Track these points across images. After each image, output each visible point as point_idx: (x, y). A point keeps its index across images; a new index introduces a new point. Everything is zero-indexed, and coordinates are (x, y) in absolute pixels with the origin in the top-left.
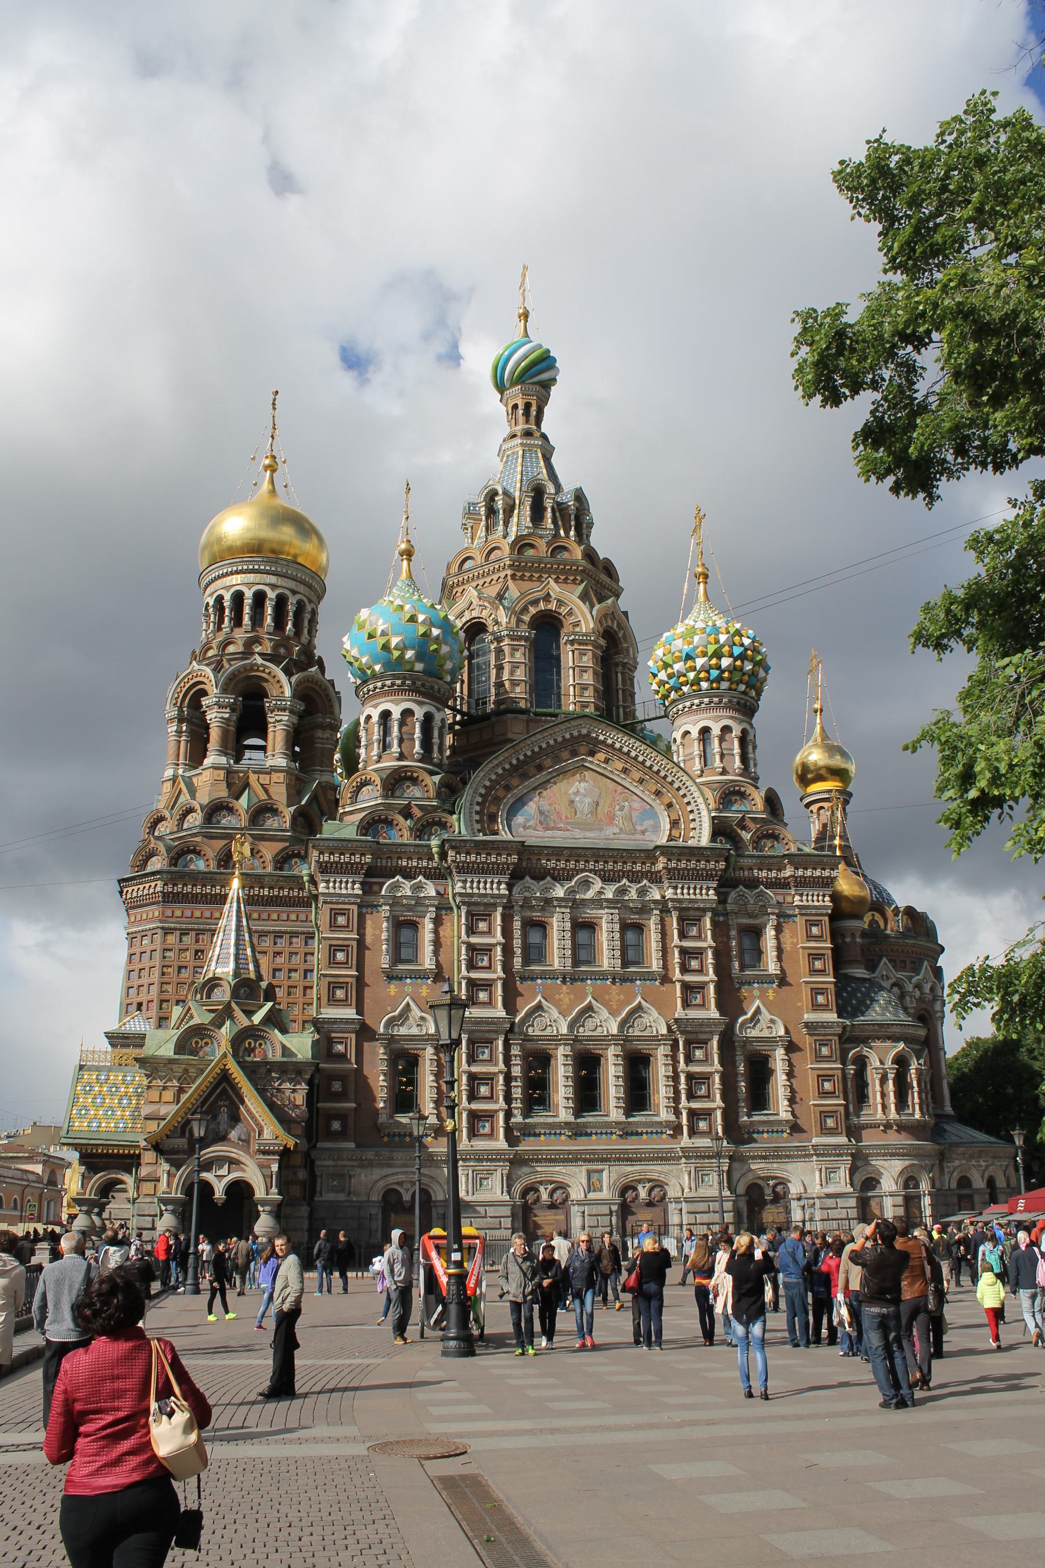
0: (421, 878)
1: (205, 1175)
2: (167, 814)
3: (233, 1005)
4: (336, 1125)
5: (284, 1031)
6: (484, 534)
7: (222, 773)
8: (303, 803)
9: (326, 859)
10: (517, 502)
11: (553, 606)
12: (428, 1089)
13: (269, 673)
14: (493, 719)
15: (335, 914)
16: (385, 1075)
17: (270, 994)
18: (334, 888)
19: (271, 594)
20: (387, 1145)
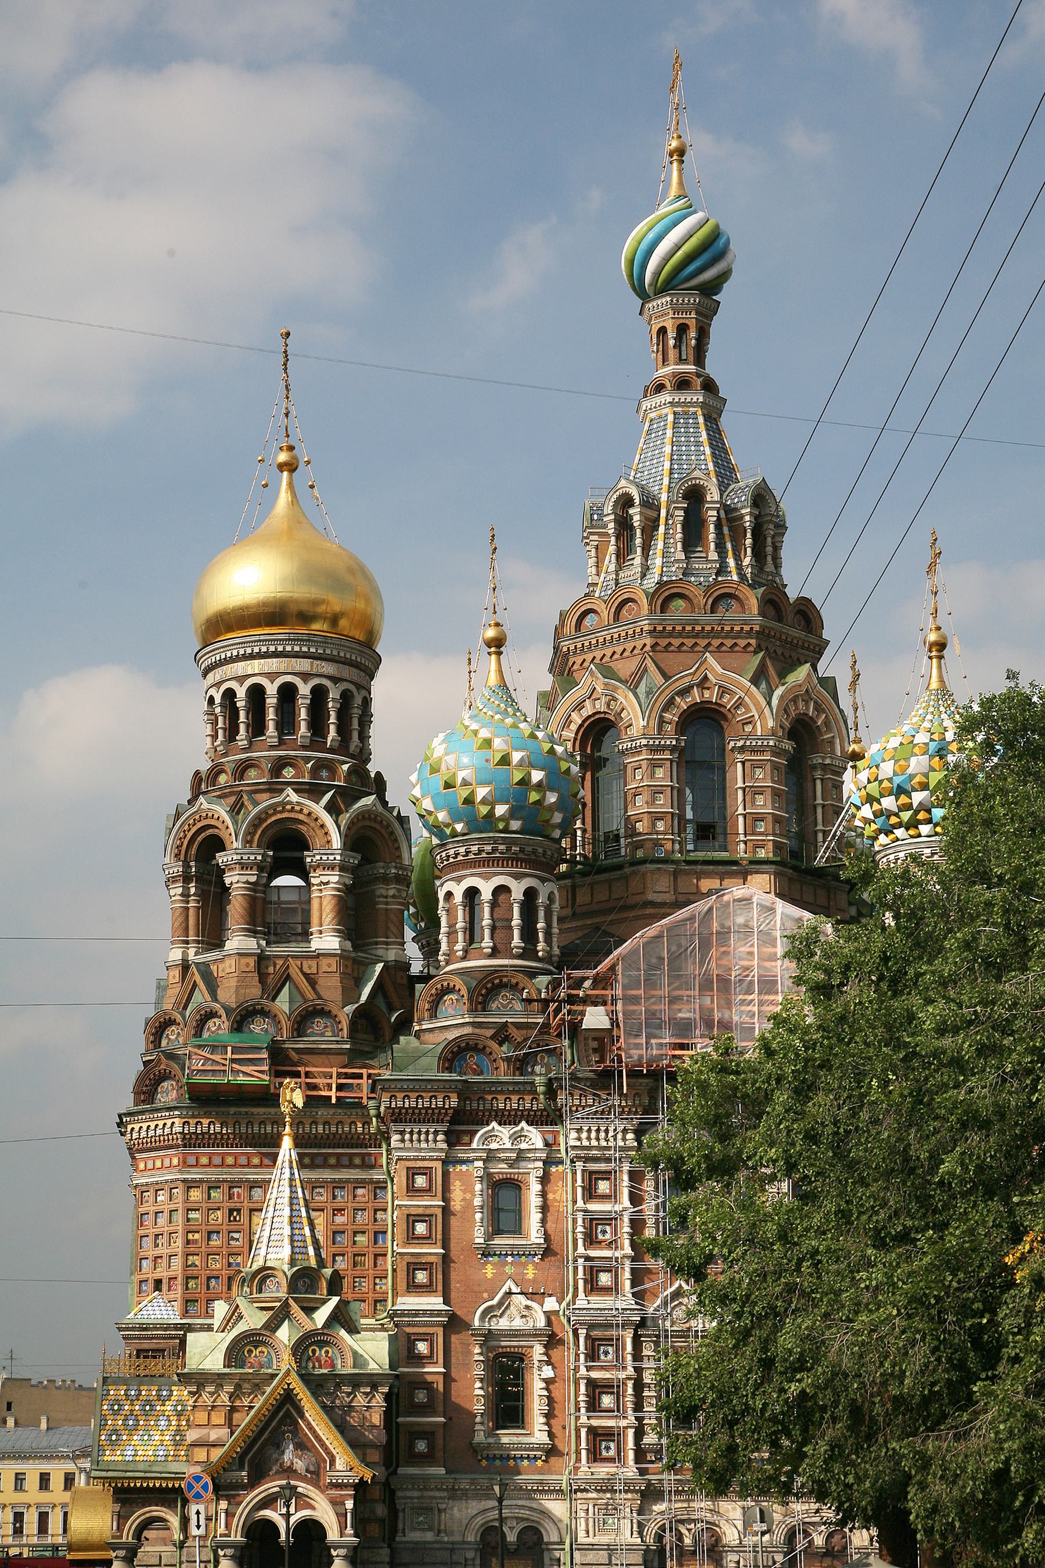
0: (523, 1124)
1: (267, 1513)
2: (179, 1018)
3: (291, 1302)
4: (421, 1446)
5: (353, 1330)
6: (612, 567)
7: (252, 961)
8: (364, 998)
9: (400, 1104)
10: (663, 513)
11: (711, 695)
12: (536, 1398)
13: (309, 814)
14: (627, 870)
15: (412, 1173)
16: (481, 1380)
17: (335, 1285)
18: (411, 1141)
19: (304, 689)
20: (486, 1471)
